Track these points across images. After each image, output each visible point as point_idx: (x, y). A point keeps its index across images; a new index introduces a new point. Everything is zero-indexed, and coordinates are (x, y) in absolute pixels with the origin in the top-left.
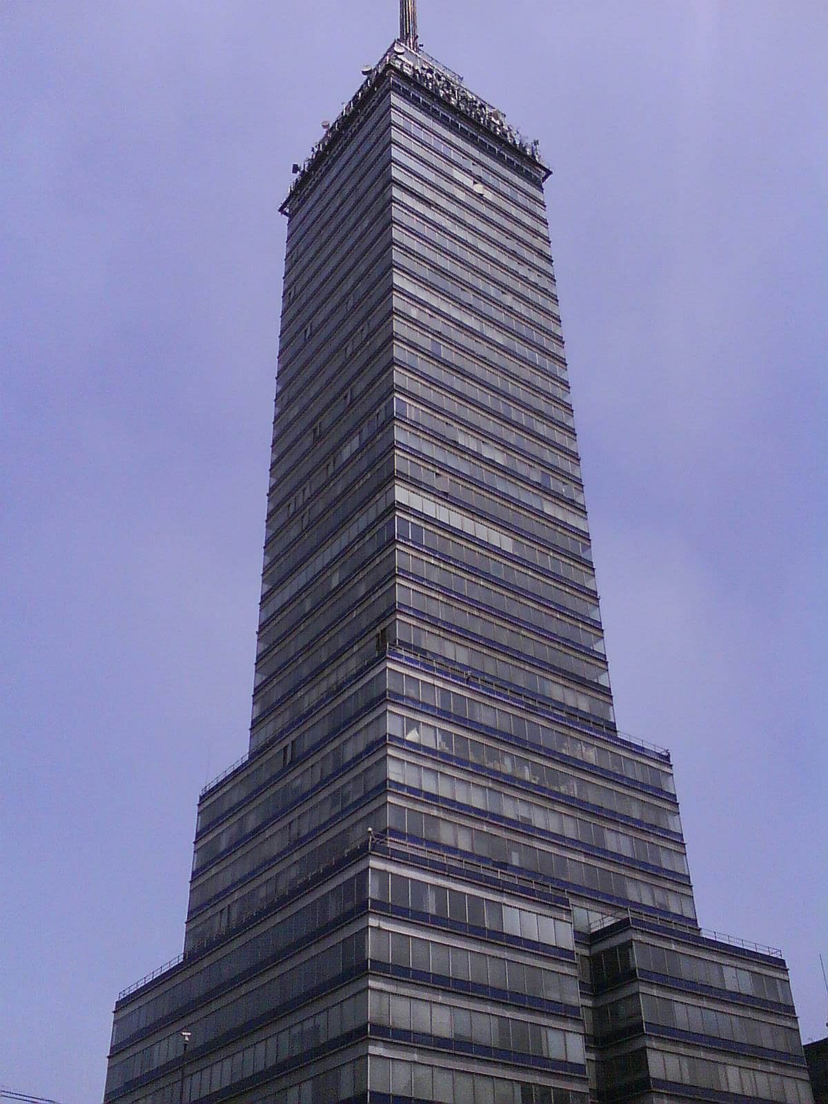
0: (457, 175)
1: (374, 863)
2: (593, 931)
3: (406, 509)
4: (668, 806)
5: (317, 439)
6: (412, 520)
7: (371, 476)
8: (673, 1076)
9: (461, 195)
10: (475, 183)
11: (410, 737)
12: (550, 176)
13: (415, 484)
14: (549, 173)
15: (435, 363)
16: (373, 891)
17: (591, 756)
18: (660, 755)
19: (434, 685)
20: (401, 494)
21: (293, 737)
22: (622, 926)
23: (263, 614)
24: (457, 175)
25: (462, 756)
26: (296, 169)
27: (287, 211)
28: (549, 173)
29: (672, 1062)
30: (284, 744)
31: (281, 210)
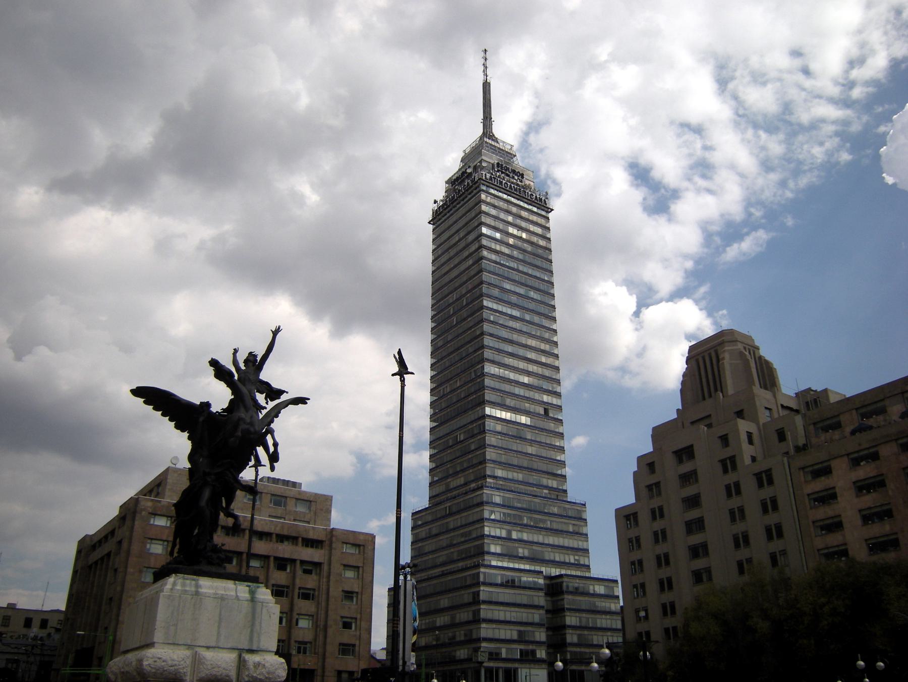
0: (511, 230)
3: (490, 416)
4: (582, 524)
8: (573, 624)
9: (511, 241)
10: (518, 230)
11: (493, 517)
12: (553, 211)
13: (494, 404)
14: (552, 210)
15: (501, 341)
16: (482, 579)
17: (555, 510)
18: (582, 504)
20: (488, 411)
22: (561, 576)
23: (432, 436)
24: (511, 230)
26: (435, 202)
29: (573, 619)
31: (429, 223)
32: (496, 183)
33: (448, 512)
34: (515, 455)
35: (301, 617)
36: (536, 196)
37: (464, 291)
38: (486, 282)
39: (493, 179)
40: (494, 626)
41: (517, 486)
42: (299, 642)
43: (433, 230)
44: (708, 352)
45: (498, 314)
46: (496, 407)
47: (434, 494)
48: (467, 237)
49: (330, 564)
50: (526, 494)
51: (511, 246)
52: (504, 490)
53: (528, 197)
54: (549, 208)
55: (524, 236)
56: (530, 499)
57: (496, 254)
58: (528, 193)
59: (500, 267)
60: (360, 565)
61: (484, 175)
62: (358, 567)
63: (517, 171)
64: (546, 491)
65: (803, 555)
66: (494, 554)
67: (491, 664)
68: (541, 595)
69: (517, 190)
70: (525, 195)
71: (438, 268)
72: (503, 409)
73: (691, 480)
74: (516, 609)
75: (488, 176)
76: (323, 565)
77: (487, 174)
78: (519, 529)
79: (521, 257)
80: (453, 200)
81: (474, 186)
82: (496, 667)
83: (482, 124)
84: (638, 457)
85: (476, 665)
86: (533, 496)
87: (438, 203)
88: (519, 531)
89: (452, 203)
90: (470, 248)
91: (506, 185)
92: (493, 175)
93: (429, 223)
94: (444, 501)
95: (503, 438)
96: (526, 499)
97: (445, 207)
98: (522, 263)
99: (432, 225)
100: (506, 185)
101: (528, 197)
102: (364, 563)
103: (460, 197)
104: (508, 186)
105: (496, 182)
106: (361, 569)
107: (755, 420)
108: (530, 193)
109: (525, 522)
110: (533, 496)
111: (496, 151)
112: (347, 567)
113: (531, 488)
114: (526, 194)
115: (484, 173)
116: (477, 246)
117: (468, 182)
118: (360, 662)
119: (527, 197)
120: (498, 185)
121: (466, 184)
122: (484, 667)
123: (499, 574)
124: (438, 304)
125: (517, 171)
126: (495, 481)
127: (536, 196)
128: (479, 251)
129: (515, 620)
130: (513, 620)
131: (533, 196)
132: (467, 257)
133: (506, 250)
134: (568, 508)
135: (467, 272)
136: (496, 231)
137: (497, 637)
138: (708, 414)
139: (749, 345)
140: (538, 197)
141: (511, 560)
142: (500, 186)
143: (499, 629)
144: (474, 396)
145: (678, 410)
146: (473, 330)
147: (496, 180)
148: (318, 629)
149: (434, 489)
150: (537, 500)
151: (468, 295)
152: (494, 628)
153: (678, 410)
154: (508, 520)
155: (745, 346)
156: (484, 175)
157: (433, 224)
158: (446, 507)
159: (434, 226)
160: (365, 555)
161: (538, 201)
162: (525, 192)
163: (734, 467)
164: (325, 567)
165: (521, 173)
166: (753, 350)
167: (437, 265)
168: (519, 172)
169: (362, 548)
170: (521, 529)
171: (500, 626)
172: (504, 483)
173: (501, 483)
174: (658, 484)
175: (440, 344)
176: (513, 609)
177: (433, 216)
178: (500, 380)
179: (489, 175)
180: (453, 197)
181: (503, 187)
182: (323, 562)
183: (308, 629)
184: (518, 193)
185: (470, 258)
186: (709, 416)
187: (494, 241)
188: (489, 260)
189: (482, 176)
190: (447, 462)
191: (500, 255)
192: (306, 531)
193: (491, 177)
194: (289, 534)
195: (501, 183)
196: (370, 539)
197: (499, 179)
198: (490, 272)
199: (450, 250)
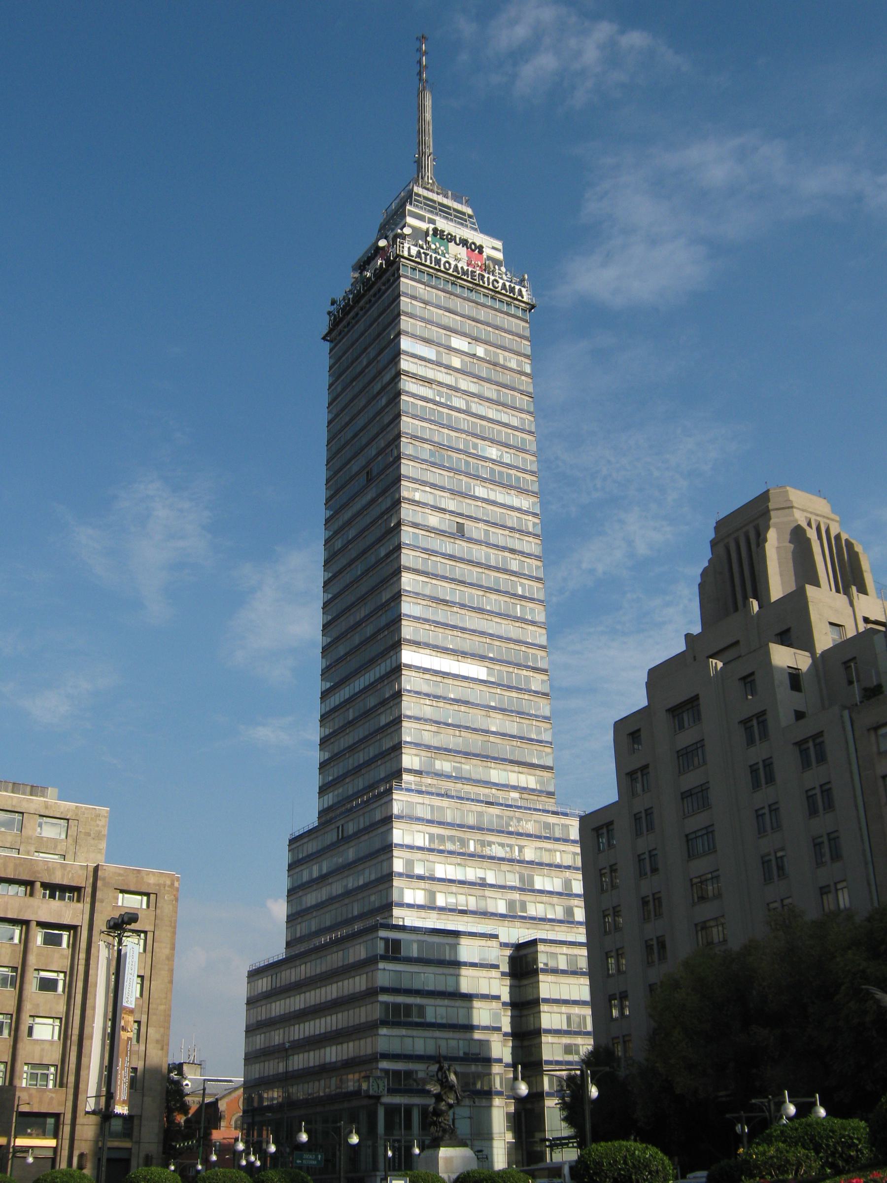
1: (383, 933)
2: (520, 942)
5: (370, 480)
6: (414, 674)
7: (388, 634)
9: (456, 362)
10: (469, 343)
15: (433, 535)
19: (424, 804)
21: (342, 822)
22: (534, 943)
23: (323, 705)
25: (442, 848)
26: (333, 303)
27: (329, 339)
29: (556, 1017)
30: (337, 825)
31: (324, 338)
32: (428, 263)
33: (340, 837)
34: (457, 733)
35: (38, 1020)
36: (504, 285)
37: (374, 452)
38: (408, 434)
39: (423, 256)
40: (403, 1032)
41: (459, 786)
42: (34, 1066)
43: (331, 350)
44: (744, 530)
45: (428, 489)
46: (422, 651)
47: (326, 806)
48: (379, 358)
50: (473, 800)
51: (456, 370)
52: (432, 794)
53: (489, 285)
55: (480, 351)
56: (479, 809)
57: (426, 384)
58: (488, 278)
59: (435, 407)
61: (406, 249)
62: (145, 932)
63: (470, 241)
64: (515, 795)
65: (873, 888)
66: (410, 906)
67: (397, 1100)
68: (494, 976)
69: (468, 274)
70: (483, 280)
71: (337, 416)
72: (434, 653)
73: (696, 759)
74: (446, 1002)
75: (414, 251)
77: (412, 247)
78: (459, 861)
79: (473, 388)
80: (358, 298)
81: (391, 270)
82: (406, 1105)
84: (616, 723)
85: (372, 1101)
86: (488, 803)
87: (338, 303)
88: (459, 864)
90: (382, 377)
91: (447, 265)
92: (423, 248)
93: (324, 338)
94: (336, 817)
95: (435, 704)
96: (474, 808)
97: (348, 308)
98: (476, 400)
99: (329, 343)
100: (447, 265)
101: (489, 285)
104: (450, 267)
105: (428, 261)
106: (150, 935)
107: (805, 642)
108: (492, 278)
109: (472, 849)
110: (488, 803)
111: (435, 208)
113: (487, 791)
114: (486, 279)
115: (408, 246)
116: (393, 372)
118: (145, 1098)
119: (486, 285)
120: (433, 265)
122: (382, 1104)
123: (415, 941)
124: (336, 478)
125: (470, 241)
126: (418, 779)
127: (504, 285)
128: (396, 380)
129: (444, 1021)
130: (439, 1021)
131: (498, 282)
132: (379, 393)
133: (449, 379)
134: (554, 824)
135: (378, 419)
136: (427, 345)
137: (408, 1051)
138: (734, 640)
139: (817, 515)
140: (508, 284)
141: (443, 917)
142: (437, 267)
143: (413, 1037)
144: (386, 633)
145: (688, 637)
146: (385, 517)
147: (428, 257)
149: (326, 797)
150: (494, 811)
151: (380, 458)
152: (404, 1036)
153: (688, 637)
154: (435, 846)
155: (809, 515)
156: (406, 249)
157: (331, 341)
158: (338, 828)
159: (332, 345)
160: (158, 911)
161: (507, 292)
162: (483, 276)
163: (764, 734)
165: (478, 244)
166: (825, 523)
167: (335, 412)
168: (474, 243)
169: (153, 897)
170: (462, 862)
171: (414, 1033)
172: (435, 782)
173: (429, 781)
174: (644, 769)
175: (338, 544)
176: (439, 1002)
178: (430, 603)
179: (417, 249)
180: (359, 291)
181: (442, 268)
183: (51, 1042)
184: (469, 279)
185: (383, 394)
186: (737, 643)
187: (423, 363)
188: (414, 396)
189: (403, 251)
190: (344, 750)
191: (434, 386)
192: (48, 870)
193: (419, 252)
194: (16, 877)
195: (438, 262)
196: (168, 882)
197: (434, 255)
198: (414, 417)
199: (354, 384)
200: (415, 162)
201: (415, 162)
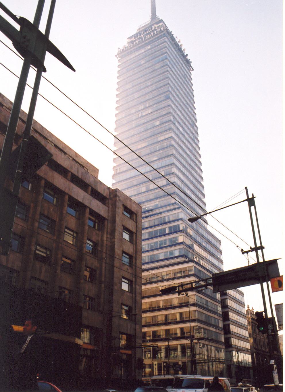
12: (193, 71)
14: (193, 70)
28: (193, 70)
31: (116, 56)
49: (114, 221)
54: (192, 69)
60: (134, 231)
76: (106, 221)
83: (150, 17)
89: (138, 44)
102: (136, 230)
103: (145, 41)
112: (126, 229)
117: (154, 33)
121: (152, 33)
148: (103, 285)
164: (108, 225)
169: (134, 216)
177: (120, 52)
182: (107, 218)
200: (150, 16)
201: (150, 16)
